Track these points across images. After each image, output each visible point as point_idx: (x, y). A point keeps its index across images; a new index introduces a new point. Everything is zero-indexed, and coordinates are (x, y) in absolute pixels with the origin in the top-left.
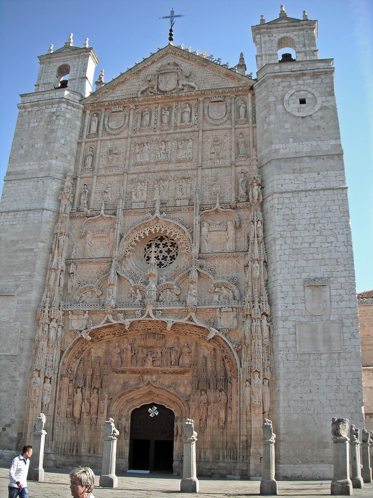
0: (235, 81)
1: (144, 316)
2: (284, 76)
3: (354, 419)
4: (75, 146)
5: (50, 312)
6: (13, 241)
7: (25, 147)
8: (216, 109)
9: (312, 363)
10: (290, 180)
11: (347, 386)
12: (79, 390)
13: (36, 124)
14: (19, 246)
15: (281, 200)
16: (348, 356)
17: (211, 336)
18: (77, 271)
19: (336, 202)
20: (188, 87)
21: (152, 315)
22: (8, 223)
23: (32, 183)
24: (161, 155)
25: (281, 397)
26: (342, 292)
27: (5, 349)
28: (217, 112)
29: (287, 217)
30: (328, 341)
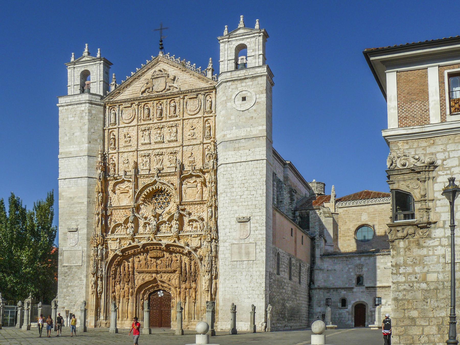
14: (76, 200)
15: (226, 169)
19: (258, 169)
27: (75, 262)
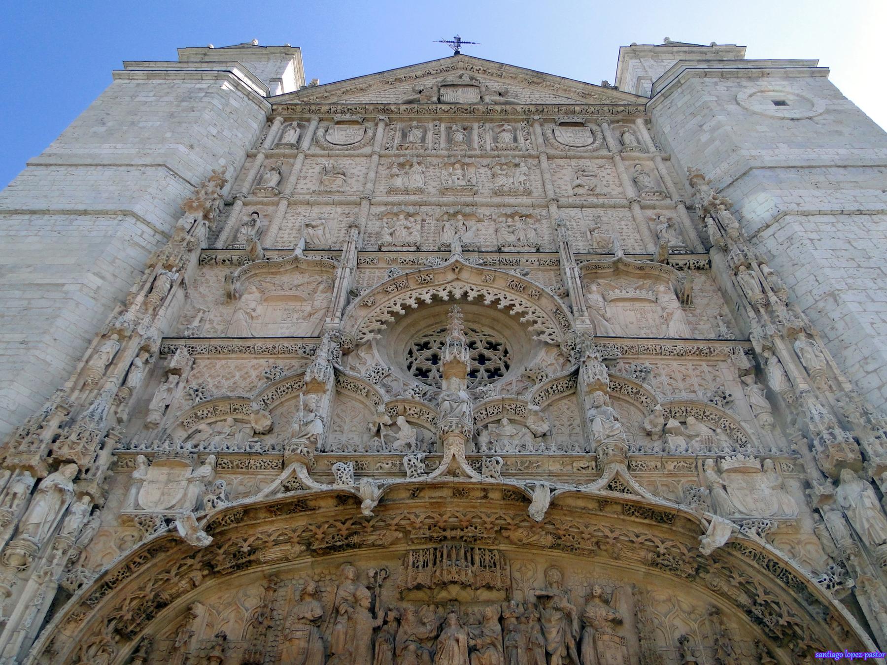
1: (437, 473)
4: (241, 154)
7: (110, 124)
18: (195, 371)
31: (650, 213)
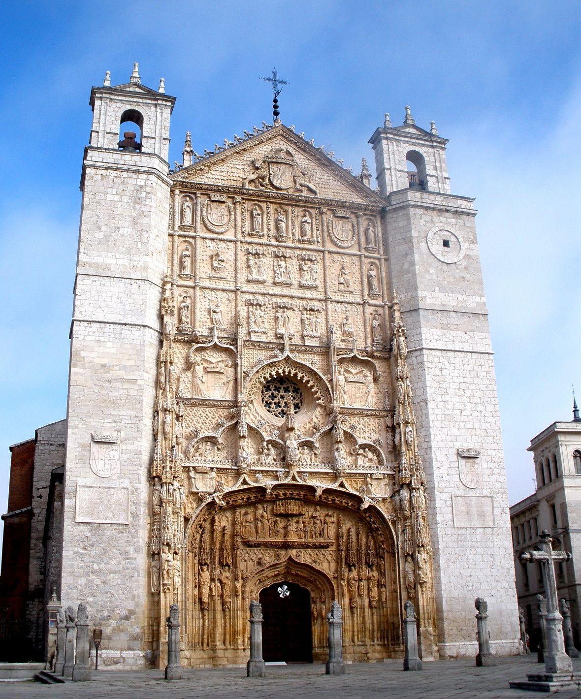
0: (361, 195)
2: (426, 208)
3: (508, 595)
5: (173, 469)
6: (103, 366)
7: (103, 228)
8: (340, 227)
9: (468, 537)
10: (438, 335)
11: (501, 562)
12: (205, 568)
13: (117, 198)
14: (115, 373)
15: (431, 358)
16: (500, 531)
17: (366, 505)
18: (186, 412)
20: (306, 188)
21: (298, 478)
22: (93, 338)
23: (122, 285)
24: (281, 275)
25: (442, 574)
26: (492, 465)
28: (342, 230)
29: (437, 378)
30: (482, 515)
31: (372, 308)
